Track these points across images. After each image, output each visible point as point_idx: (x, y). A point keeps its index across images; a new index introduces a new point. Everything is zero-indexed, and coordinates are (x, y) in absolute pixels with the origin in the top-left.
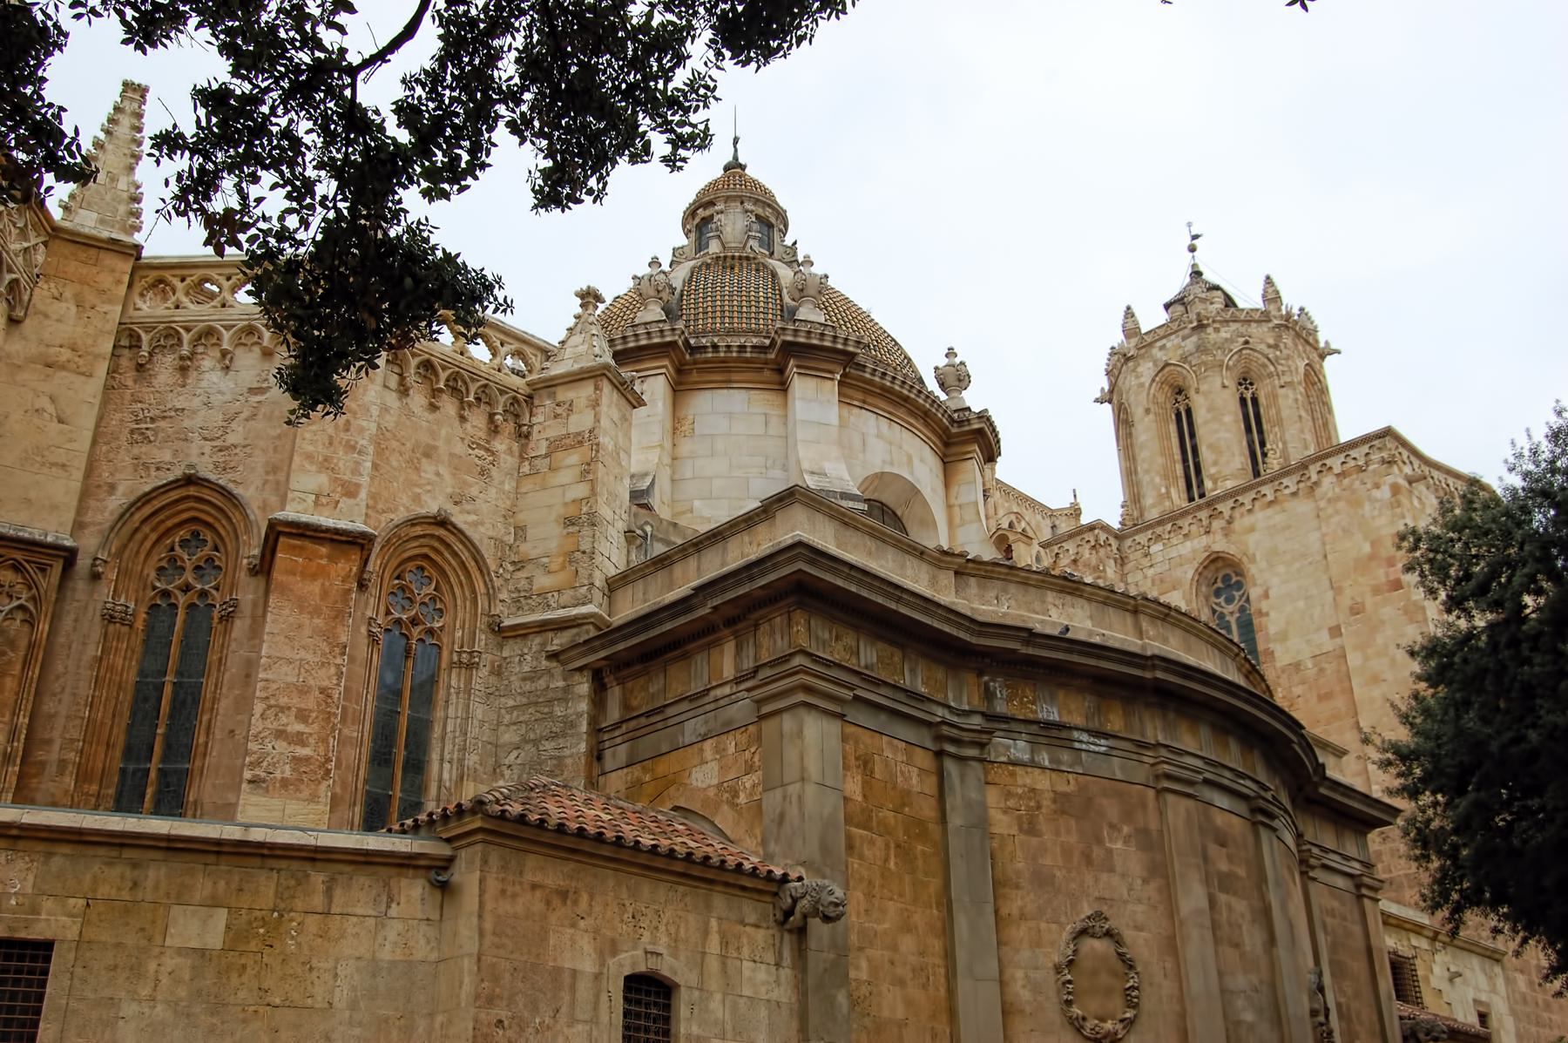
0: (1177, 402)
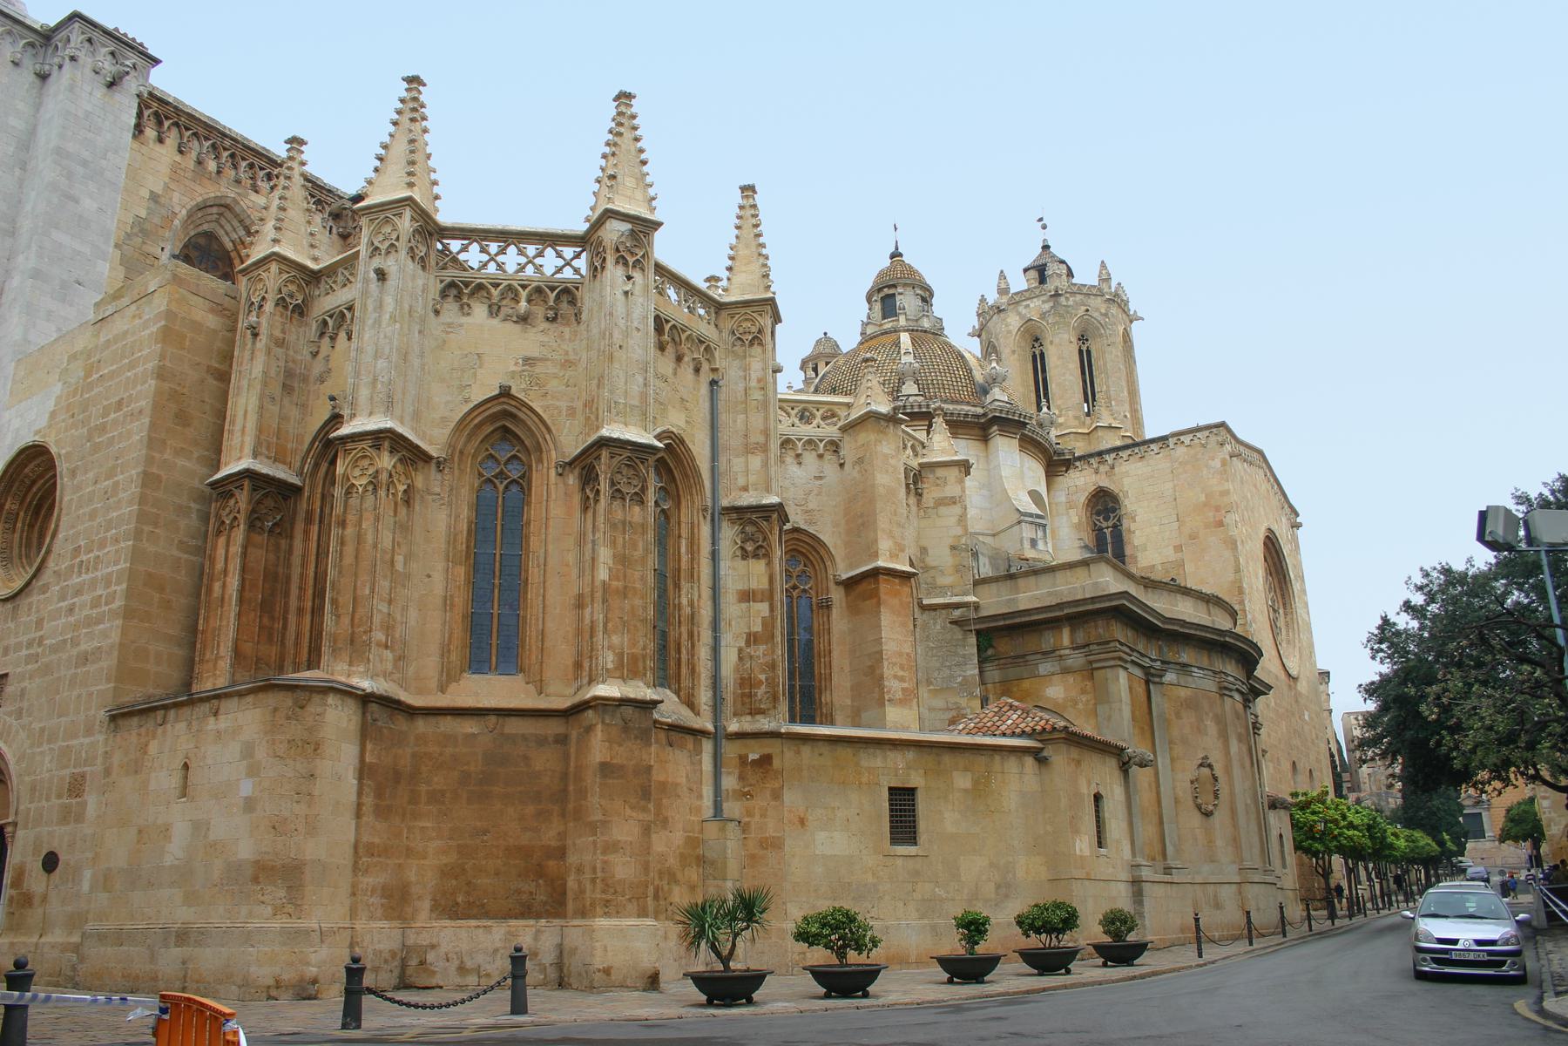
0: (1034, 347)
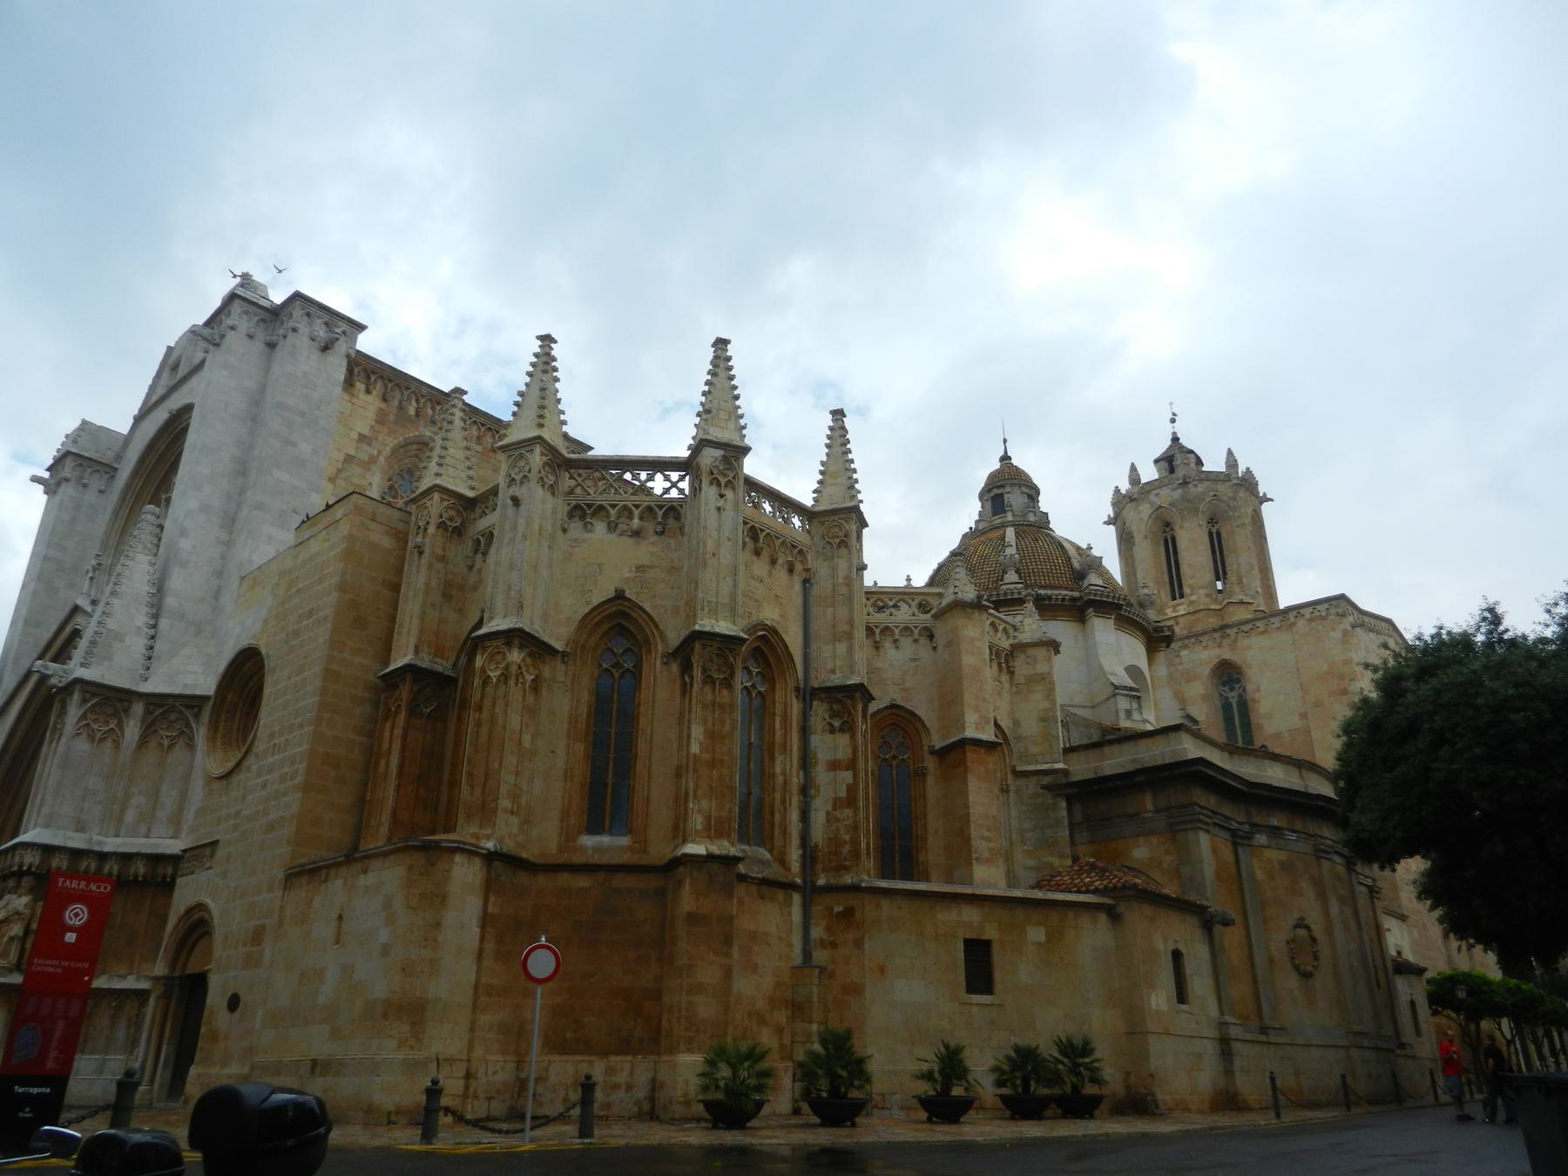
0: (1165, 532)
